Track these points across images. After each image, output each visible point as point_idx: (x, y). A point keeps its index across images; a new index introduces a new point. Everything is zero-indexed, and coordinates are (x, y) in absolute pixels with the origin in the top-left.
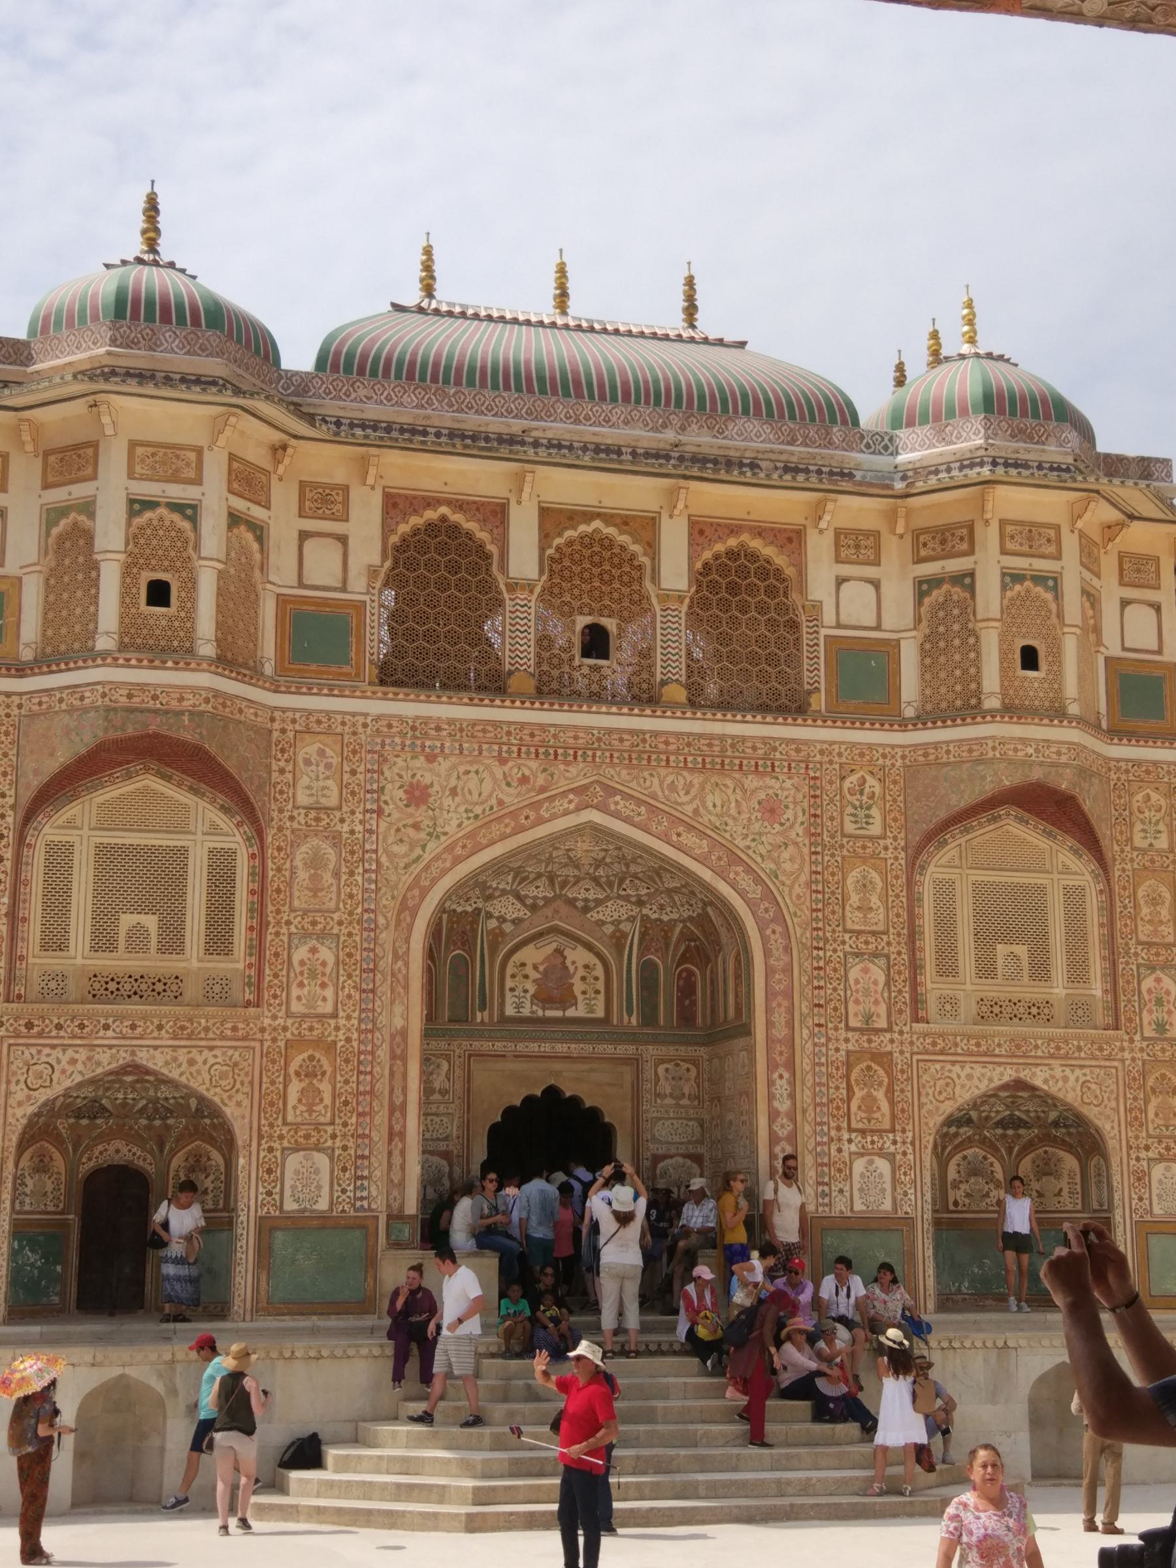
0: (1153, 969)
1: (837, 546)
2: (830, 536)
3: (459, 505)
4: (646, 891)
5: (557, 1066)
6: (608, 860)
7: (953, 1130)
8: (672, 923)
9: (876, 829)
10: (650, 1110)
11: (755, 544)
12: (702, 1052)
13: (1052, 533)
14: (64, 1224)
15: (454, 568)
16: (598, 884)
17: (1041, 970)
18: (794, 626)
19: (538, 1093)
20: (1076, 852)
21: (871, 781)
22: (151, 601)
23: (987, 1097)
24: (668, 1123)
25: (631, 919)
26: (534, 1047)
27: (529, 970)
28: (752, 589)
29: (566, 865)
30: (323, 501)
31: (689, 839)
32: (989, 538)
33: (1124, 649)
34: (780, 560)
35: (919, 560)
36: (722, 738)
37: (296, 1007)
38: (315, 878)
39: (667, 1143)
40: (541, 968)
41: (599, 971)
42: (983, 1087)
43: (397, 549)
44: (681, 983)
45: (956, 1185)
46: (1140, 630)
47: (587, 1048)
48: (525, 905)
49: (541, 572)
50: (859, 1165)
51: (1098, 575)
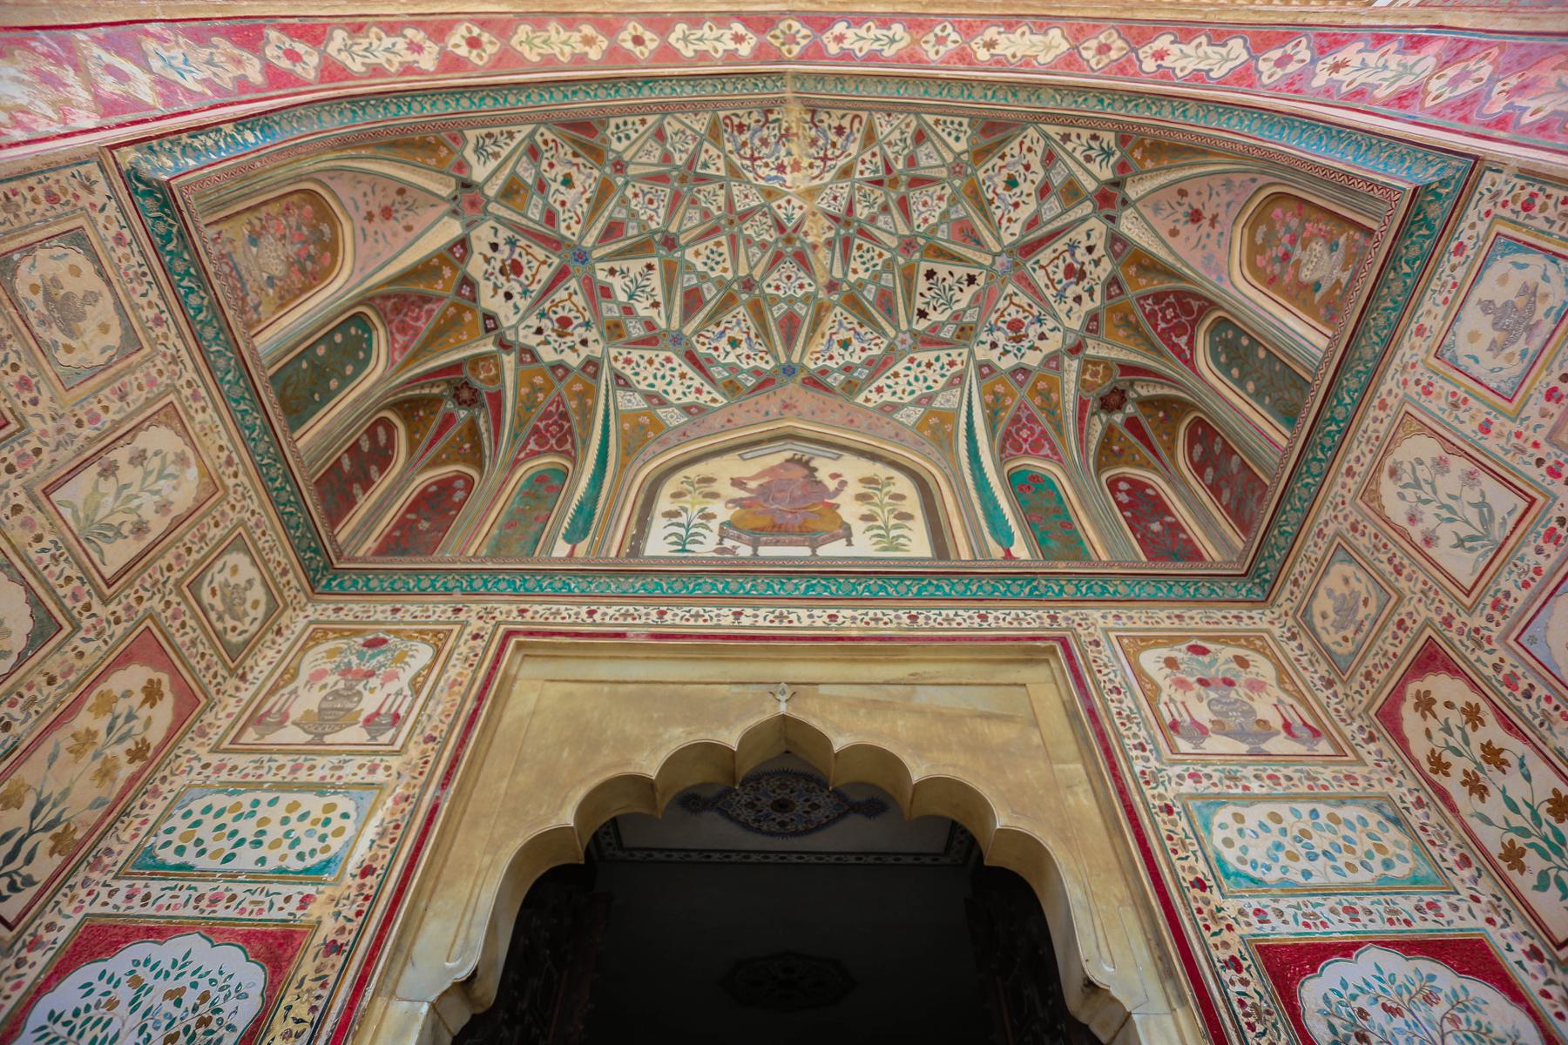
4: (970, 291)
6: (862, 212)
8: (1053, 359)
10: (1164, 779)
12: (1260, 620)
16: (866, 319)
19: (731, 738)
24: (1255, 814)
25: (958, 380)
26: (722, 618)
29: (778, 257)
39: (1288, 889)
40: (753, 485)
41: (903, 485)
44: (1124, 498)
48: (712, 381)
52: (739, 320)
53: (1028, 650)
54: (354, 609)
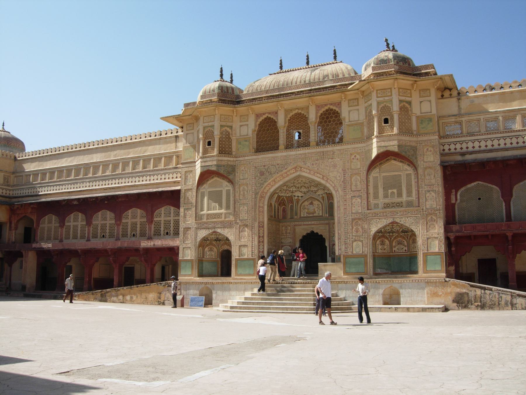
0: (429, 191)
1: (349, 103)
2: (347, 101)
3: (269, 113)
5: (313, 226)
7: (391, 234)
9: (359, 167)
11: (331, 107)
13: (389, 90)
14: (218, 261)
15: (270, 126)
17: (400, 195)
18: (341, 123)
20: (409, 165)
21: (358, 156)
22: (208, 145)
23: (386, 226)
26: (307, 223)
27: (306, 207)
28: (332, 117)
30: (244, 117)
31: (318, 175)
32: (374, 94)
33: (421, 113)
34: (337, 109)
35: (366, 103)
36: (323, 152)
37: (241, 218)
38: (244, 193)
41: (321, 206)
42: (385, 224)
43: (259, 125)
45: (395, 247)
46: (426, 107)
47: (318, 222)
49: (285, 123)
50: (355, 244)
51: (411, 97)
52: (303, 188)
53: (327, 224)
54: (283, 224)
